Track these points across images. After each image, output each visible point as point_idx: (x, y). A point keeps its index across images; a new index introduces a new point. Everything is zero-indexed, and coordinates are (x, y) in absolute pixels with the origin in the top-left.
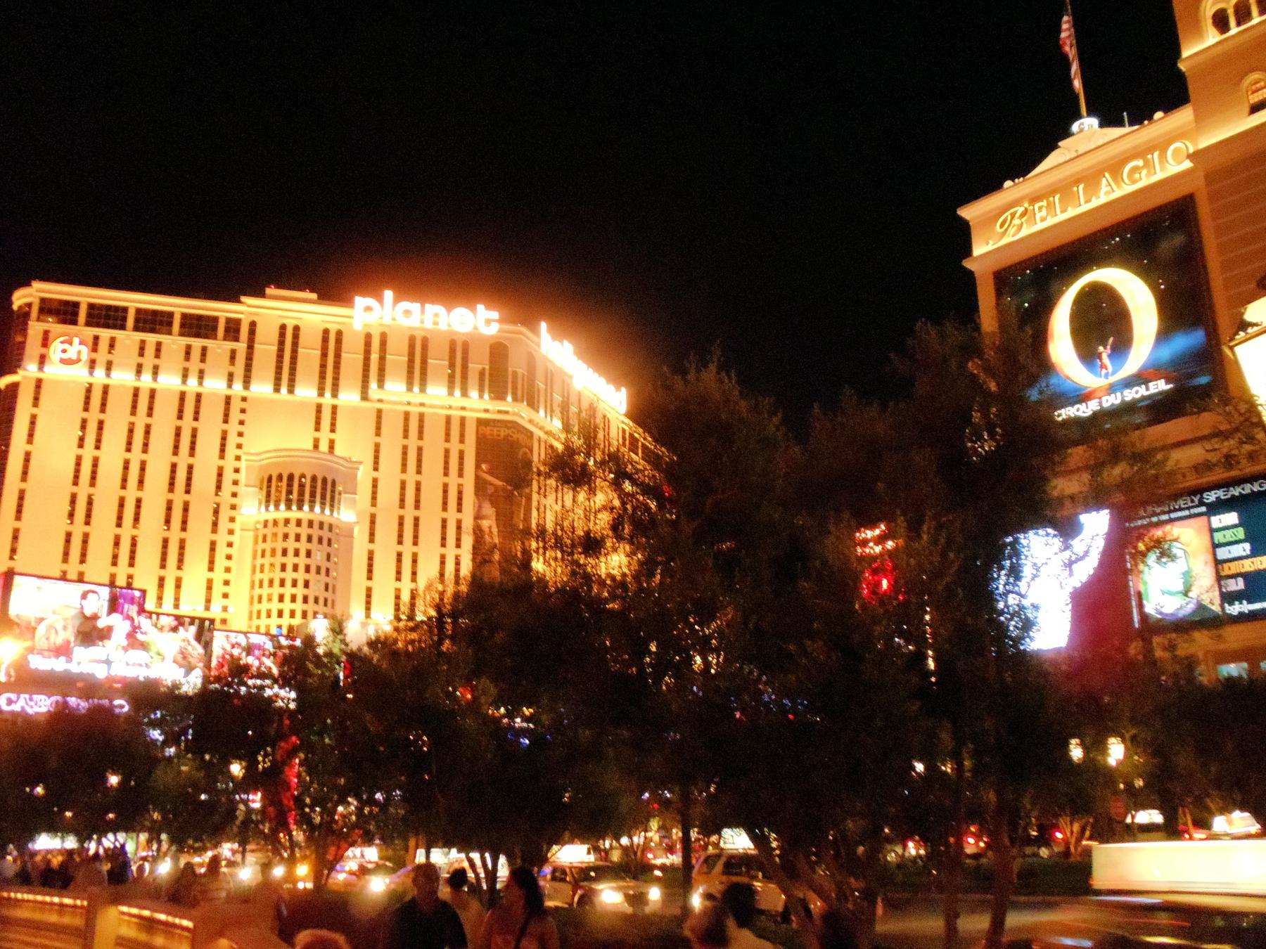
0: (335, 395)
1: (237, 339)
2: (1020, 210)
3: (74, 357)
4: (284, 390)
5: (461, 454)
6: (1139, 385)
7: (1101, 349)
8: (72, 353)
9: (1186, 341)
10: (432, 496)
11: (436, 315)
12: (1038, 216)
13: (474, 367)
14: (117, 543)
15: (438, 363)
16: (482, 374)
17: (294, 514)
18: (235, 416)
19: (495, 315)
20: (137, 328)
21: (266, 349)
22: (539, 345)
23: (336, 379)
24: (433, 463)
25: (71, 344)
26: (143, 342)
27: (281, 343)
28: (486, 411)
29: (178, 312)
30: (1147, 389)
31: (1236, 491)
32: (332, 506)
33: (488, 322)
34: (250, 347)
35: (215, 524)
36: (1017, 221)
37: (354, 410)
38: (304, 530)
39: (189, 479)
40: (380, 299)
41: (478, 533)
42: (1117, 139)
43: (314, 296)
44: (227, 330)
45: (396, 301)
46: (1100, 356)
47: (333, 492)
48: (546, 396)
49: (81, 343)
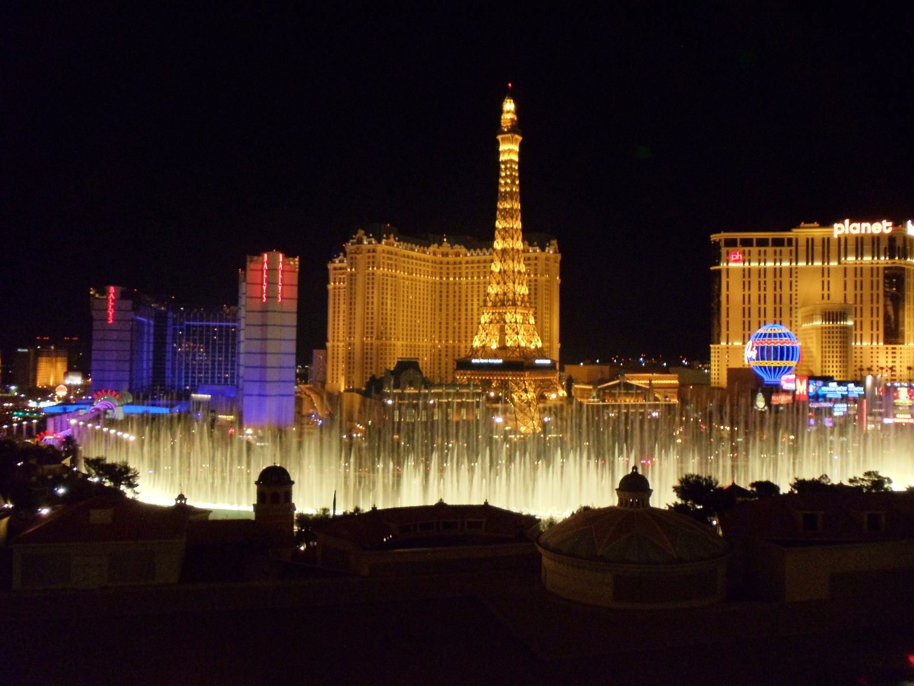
4: (810, 264)
8: (737, 257)
11: (866, 228)
13: (882, 247)
15: (867, 247)
16: (885, 249)
18: (794, 275)
19: (890, 224)
21: (802, 249)
27: (808, 246)
33: (887, 228)
35: (791, 315)
37: (834, 268)
39: (781, 299)
43: (818, 225)
45: (851, 223)
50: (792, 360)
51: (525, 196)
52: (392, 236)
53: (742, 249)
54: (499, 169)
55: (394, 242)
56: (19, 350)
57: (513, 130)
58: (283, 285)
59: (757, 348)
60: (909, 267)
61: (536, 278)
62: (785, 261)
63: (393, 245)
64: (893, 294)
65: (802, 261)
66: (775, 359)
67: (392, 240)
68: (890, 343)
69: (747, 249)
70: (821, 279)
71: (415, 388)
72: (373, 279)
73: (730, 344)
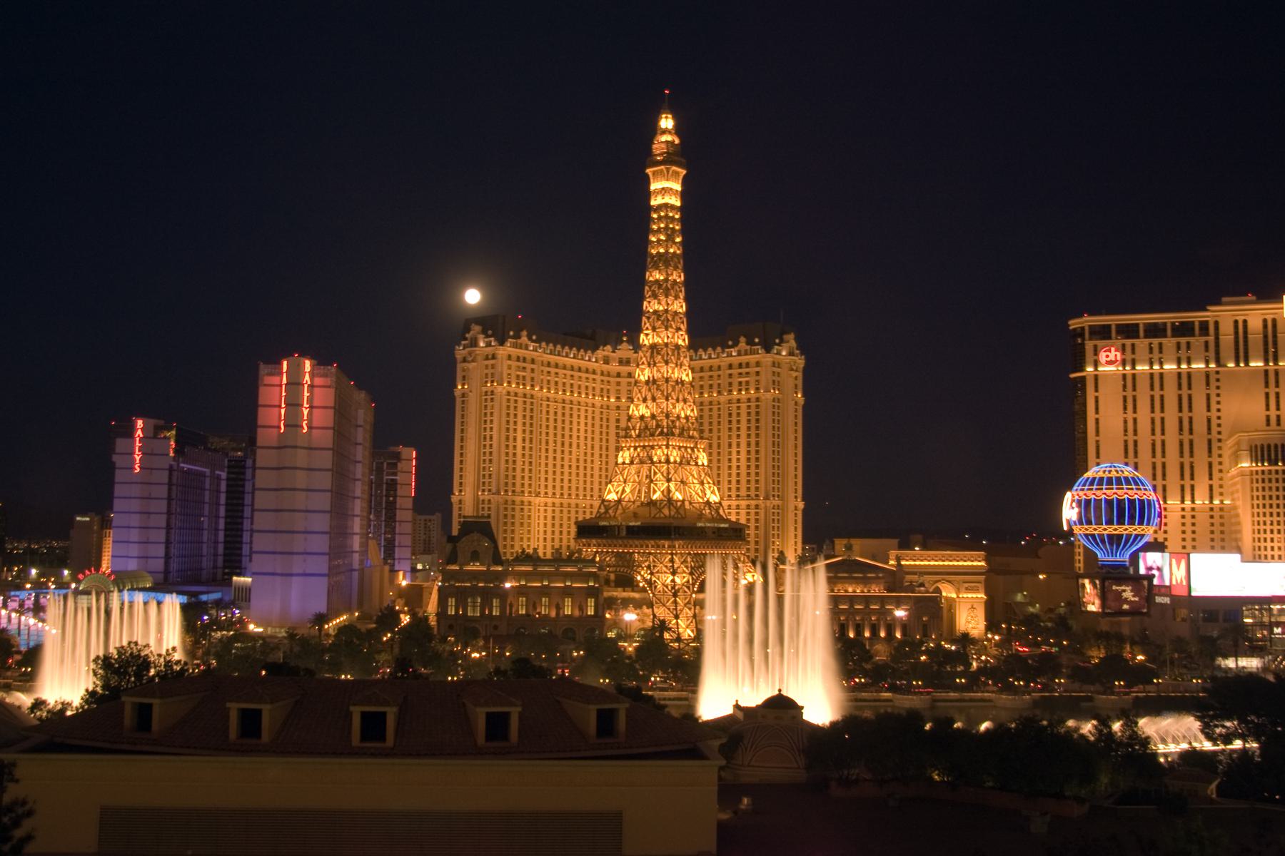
1: (1207, 335)
3: (1114, 359)
8: (1112, 357)
18: (1213, 383)
21: (1227, 339)
25: (1110, 352)
35: (1210, 451)
43: (1254, 298)
49: (1116, 351)
50: (1148, 524)
51: (692, 259)
52: (524, 333)
53: (1120, 342)
54: (649, 220)
55: (529, 343)
56: (78, 519)
57: (669, 160)
58: (311, 407)
59: (1079, 502)
61: (757, 395)
63: (527, 348)
66: (1109, 522)
67: (524, 339)
69: (1128, 342)
70: (1263, 391)
71: (481, 564)
72: (492, 399)
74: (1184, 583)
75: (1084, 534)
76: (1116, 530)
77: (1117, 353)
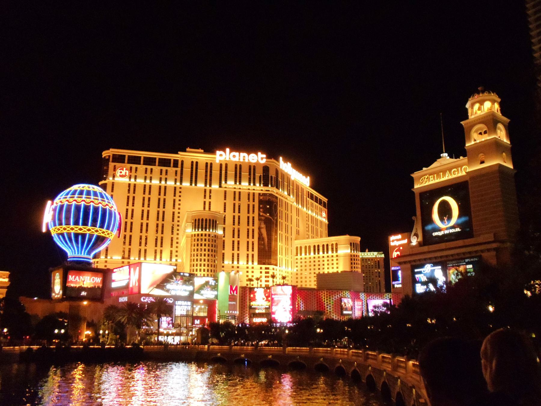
0: (210, 186)
1: (177, 167)
2: (426, 177)
3: (124, 174)
4: (193, 185)
5: (254, 206)
6: (453, 229)
7: (445, 218)
8: (123, 173)
9: (463, 219)
10: (244, 220)
11: (244, 157)
12: (431, 179)
13: (257, 175)
14: (141, 238)
15: (245, 174)
16: (260, 177)
17: (204, 232)
18: (178, 194)
19: (264, 156)
20: (144, 164)
21: (187, 170)
22: (279, 165)
23: (211, 180)
24: (244, 209)
26: (146, 169)
27: (192, 168)
28: (262, 190)
29: (158, 157)
30: (455, 230)
31: (472, 260)
32: (216, 229)
33: (262, 159)
34: (182, 170)
35: (172, 232)
36: (425, 180)
37: (216, 191)
38: (207, 238)
40: (225, 151)
41: (260, 234)
42: (452, 163)
43: (202, 151)
44: (174, 164)
45: (231, 152)
46: (444, 220)
47: (216, 224)
48: (282, 184)
49: (126, 170)
60: (281, 198)
62: (171, 180)
64: (266, 218)
65: (186, 181)
66: (76, 223)
68: (264, 264)
73: (109, 257)
74: (137, 285)
75: (57, 234)
76: (81, 229)
77: (127, 171)
